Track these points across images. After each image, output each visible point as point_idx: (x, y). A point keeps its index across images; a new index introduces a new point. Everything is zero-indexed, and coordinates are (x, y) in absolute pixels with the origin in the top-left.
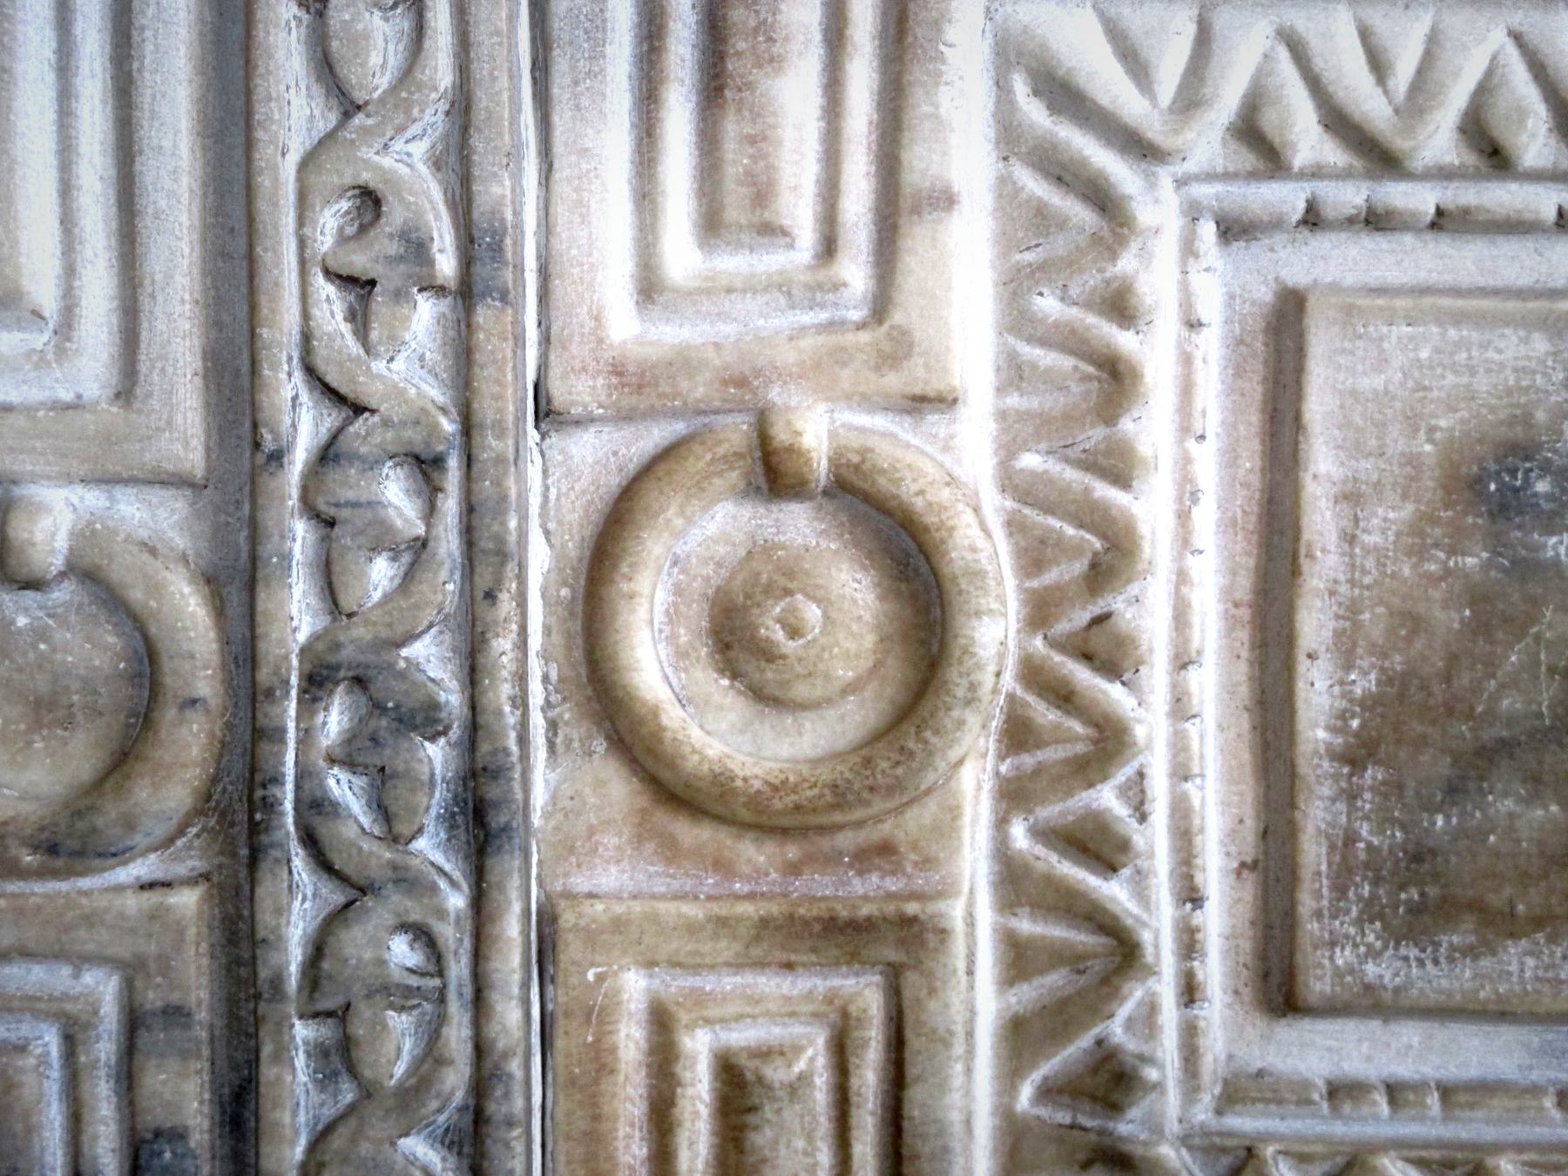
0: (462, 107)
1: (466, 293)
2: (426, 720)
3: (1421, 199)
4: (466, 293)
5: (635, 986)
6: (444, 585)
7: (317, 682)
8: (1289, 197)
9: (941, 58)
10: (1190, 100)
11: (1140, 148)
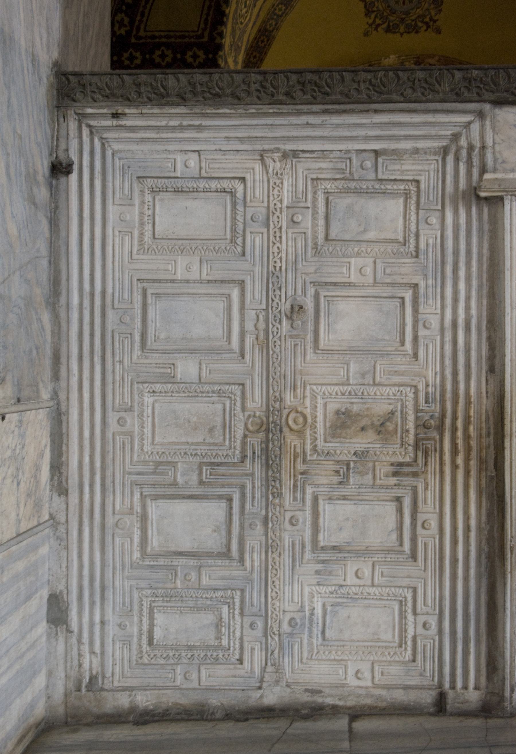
0: (281, 391)
1: (281, 402)
2: (278, 425)
3: (333, 397)
4: (281, 402)
5: (289, 441)
6: (279, 418)
7: (272, 423)
8: (326, 397)
10: (321, 391)
11: (318, 394)
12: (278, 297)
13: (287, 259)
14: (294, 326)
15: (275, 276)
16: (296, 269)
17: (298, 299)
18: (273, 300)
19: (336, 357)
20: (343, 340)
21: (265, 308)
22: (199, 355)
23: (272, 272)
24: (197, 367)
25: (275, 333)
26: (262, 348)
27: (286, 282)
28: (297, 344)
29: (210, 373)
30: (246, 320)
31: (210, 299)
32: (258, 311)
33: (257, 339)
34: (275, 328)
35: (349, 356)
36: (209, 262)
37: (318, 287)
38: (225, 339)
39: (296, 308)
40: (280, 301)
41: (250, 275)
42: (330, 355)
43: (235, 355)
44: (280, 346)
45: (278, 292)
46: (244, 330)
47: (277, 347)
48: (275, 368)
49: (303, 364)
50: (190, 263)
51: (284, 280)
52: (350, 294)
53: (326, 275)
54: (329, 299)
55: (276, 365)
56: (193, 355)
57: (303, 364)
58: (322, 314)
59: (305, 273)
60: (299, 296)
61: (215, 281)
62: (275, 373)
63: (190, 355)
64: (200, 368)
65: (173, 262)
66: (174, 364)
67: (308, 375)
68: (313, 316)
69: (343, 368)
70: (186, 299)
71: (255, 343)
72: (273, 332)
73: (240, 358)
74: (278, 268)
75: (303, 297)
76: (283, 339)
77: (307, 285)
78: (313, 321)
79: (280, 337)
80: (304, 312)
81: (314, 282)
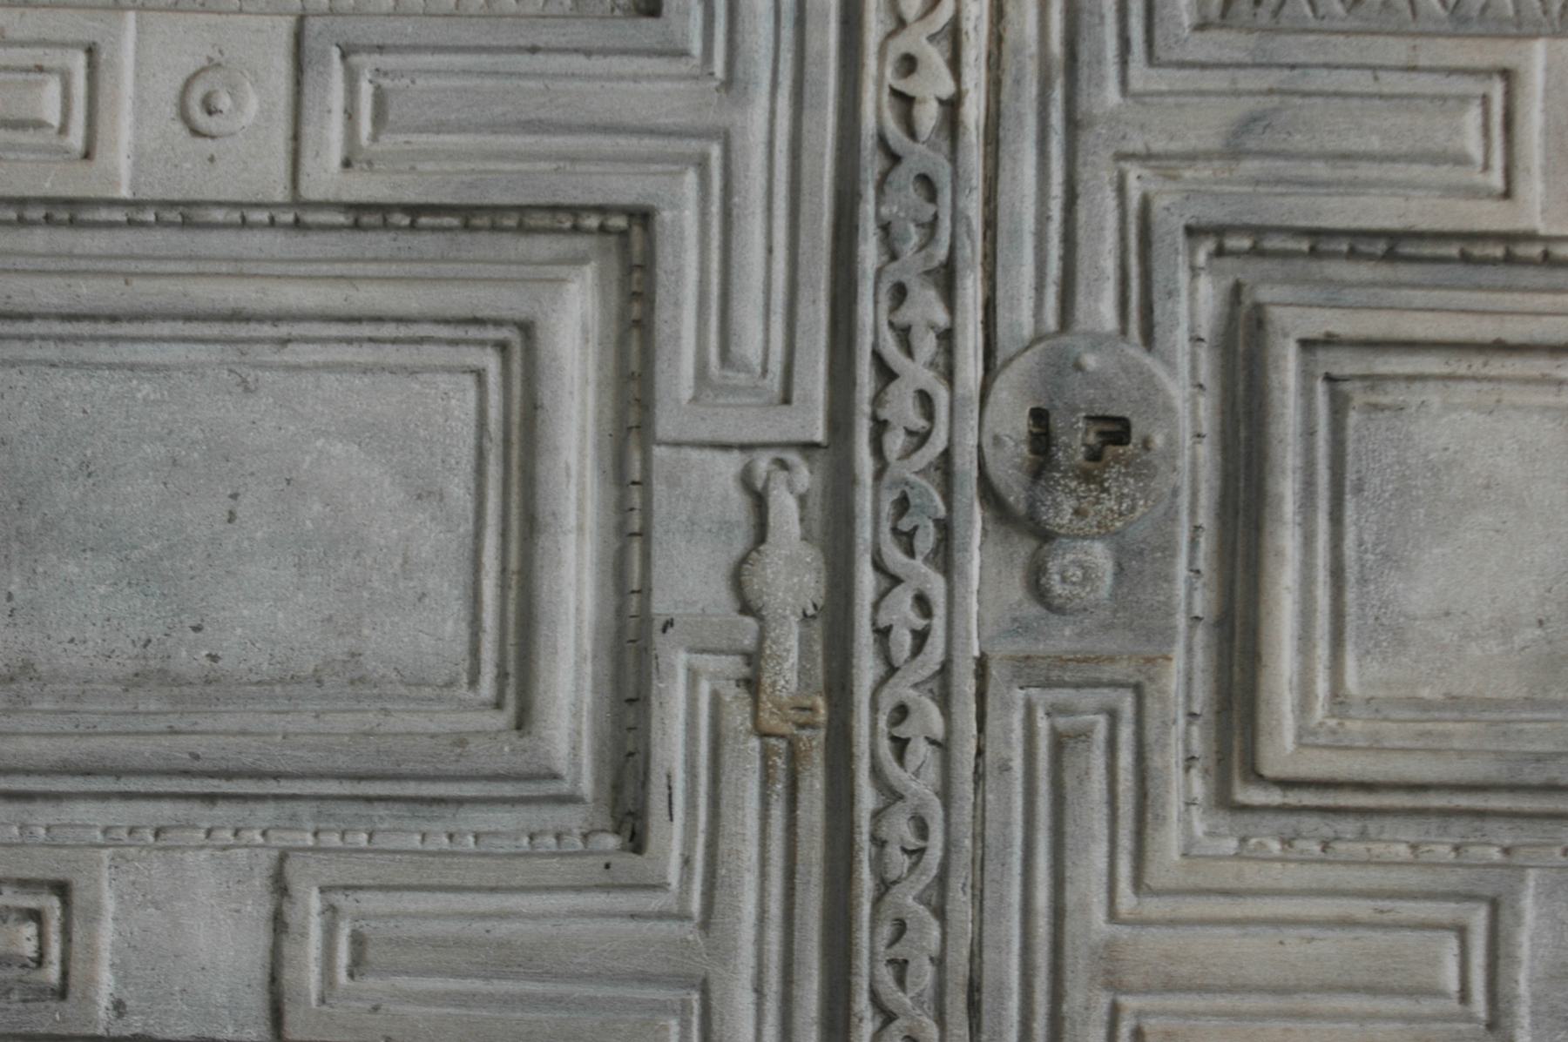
12: (927, 346)
13: (997, 39)
14: (1057, 588)
15: (904, 175)
16: (1073, 124)
17: (1091, 361)
18: (886, 373)
19: (1395, 841)
20: (1456, 704)
21: (819, 435)
22: (267, 812)
23: (882, 140)
24: (258, 908)
25: (902, 641)
26: (793, 756)
27: (990, 224)
28: (1084, 735)
29: (357, 966)
30: (657, 533)
31: (367, 354)
32: (763, 462)
33: (751, 685)
34: (902, 601)
35: (1505, 834)
36: (366, 63)
37: (1250, 271)
38: (487, 687)
39: (1075, 441)
40: (949, 375)
41: (702, 164)
42: (1349, 826)
43: (572, 818)
44: (943, 746)
45: (926, 307)
46: (645, 617)
47: (920, 751)
48: (901, 927)
49: (1126, 899)
50: (213, 65)
51: (974, 207)
52: (1514, 330)
53: (1320, 170)
54: (1347, 364)
55: (907, 899)
56: (222, 810)
57: (1126, 899)
58: (1286, 489)
59: (1146, 157)
60: (1097, 341)
61: (415, 210)
62: (900, 967)
63: (197, 810)
64: (279, 923)
65: (79, 62)
66: (62, 890)
67: (1170, 986)
68: (1207, 500)
69: (1462, 932)
70: (177, 352)
71: (738, 715)
72: (883, 634)
73: (611, 842)
74: (928, 116)
75: (1133, 350)
76: (966, 685)
77: (1160, 250)
78: (1205, 544)
79: (945, 670)
80: (1142, 470)
81: (1220, 231)
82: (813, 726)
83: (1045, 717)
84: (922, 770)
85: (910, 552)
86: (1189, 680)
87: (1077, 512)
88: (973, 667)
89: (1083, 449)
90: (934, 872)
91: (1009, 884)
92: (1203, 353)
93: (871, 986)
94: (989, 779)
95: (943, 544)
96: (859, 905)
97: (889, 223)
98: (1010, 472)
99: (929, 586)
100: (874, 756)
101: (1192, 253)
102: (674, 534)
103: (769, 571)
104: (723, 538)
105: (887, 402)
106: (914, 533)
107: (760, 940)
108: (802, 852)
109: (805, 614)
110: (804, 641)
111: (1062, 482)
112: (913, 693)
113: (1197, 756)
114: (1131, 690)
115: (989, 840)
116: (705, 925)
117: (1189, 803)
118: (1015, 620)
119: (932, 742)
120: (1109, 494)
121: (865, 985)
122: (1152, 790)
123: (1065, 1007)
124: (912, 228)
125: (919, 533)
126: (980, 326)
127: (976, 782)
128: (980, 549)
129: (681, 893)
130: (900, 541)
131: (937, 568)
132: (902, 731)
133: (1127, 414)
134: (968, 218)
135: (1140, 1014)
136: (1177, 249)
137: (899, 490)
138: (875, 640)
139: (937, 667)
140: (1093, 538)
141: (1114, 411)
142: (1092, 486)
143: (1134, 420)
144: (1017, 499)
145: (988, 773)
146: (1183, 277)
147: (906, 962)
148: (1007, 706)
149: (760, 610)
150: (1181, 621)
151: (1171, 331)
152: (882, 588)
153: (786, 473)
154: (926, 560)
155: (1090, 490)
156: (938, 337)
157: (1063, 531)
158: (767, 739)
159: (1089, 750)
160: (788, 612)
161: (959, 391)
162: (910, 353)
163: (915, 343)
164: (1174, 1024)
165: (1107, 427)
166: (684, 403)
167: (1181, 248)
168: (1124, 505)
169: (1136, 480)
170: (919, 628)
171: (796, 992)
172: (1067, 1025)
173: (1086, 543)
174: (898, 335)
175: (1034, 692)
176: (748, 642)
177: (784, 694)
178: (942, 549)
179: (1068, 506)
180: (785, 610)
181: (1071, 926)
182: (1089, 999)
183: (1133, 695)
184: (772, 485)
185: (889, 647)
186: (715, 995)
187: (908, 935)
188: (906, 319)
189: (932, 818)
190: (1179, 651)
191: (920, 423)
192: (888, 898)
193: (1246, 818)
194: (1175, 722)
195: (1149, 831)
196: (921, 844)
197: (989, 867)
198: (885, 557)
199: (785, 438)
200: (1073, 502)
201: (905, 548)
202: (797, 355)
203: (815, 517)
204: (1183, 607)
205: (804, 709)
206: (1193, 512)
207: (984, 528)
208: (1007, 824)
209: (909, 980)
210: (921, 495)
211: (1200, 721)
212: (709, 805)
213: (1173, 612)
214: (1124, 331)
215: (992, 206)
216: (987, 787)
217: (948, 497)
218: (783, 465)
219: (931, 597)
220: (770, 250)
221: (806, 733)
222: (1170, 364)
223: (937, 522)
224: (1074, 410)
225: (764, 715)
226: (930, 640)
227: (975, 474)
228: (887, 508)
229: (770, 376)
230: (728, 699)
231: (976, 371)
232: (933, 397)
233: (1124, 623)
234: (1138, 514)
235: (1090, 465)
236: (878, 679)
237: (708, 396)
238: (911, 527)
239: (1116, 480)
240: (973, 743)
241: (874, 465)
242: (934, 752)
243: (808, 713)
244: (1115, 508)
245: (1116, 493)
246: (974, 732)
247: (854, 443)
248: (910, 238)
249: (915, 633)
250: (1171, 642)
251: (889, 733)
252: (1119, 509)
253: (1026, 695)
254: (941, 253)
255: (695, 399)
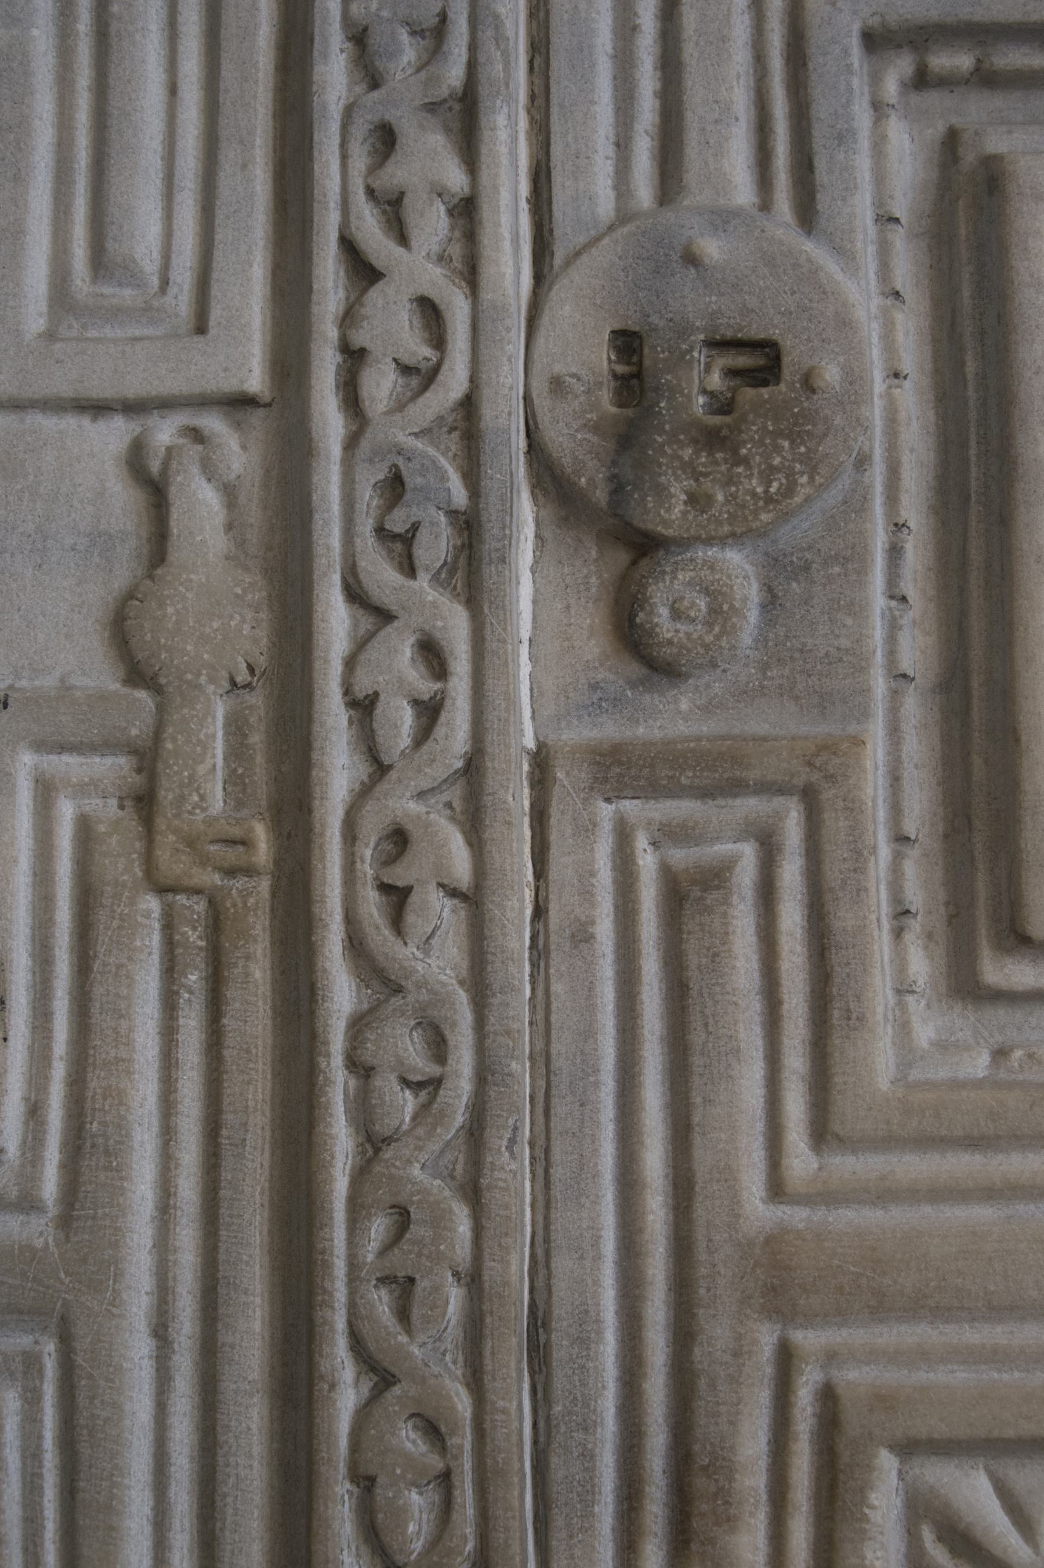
9: (865, 1519)
48: (403, 1218)
82: (249, 871)
83: (650, 849)
84: (433, 942)
85: (410, 570)
86: (895, 779)
87: (692, 499)
88: (526, 767)
89: (701, 400)
90: (460, 1119)
91: (594, 1139)
92: (899, 239)
93: (350, 1324)
94: (555, 957)
95: (466, 552)
96: (330, 1180)
97: (365, 29)
98: (579, 436)
99: (440, 624)
100: (351, 919)
101: (875, 80)
102: (13, 555)
103: (170, 610)
104: (97, 559)
105: (365, 318)
106: (414, 536)
107: (163, 1246)
108: (231, 1089)
109: (233, 683)
110: (236, 727)
111: (669, 451)
112: (414, 807)
113: (913, 910)
114: (795, 798)
115: (559, 1063)
116: (66, 1221)
117: (903, 990)
118: (594, 687)
119: (453, 893)
120: (748, 466)
121: (341, 1324)
122: (837, 969)
123: (697, 1351)
124: (404, 37)
125: (423, 536)
126: (524, 206)
127: (535, 965)
128: (533, 572)
129: (23, 1166)
130: (390, 551)
131: (455, 595)
132: (400, 875)
133: (775, 334)
134: (497, 17)
135: (831, 1357)
136: (849, 66)
137: (387, 463)
138: (351, 722)
139: (459, 764)
140: (722, 541)
141: (755, 332)
142: (719, 456)
143: (787, 343)
144: (591, 480)
145: (553, 947)
146: (863, 118)
147: (412, 1280)
148: (587, 830)
149: (154, 677)
150: (879, 685)
151: (844, 199)
152: (362, 632)
153: (200, 448)
154: (435, 578)
155: (716, 463)
156: (450, 213)
157: (670, 532)
158: (170, 896)
159: (726, 902)
160: (203, 679)
161: (486, 296)
162: (403, 240)
163: (411, 218)
164: (891, 1376)
165: (742, 360)
166: (28, 337)
167: (856, 65)
168: (775, 485)
169: (792, 442)
170: (426, 697)
171: (225, 1337)
172: (702, 1383)
173: (712, 552)
174: (384, 212)
175: (630, 807)
176: (138, 730)
177: (200, 816)
178: (462, 561)
179: (678, 490)
180: (199, 674)
181: (701, 1212)
182: (739, 1337)
183: (802, 808)
184: (174, 465)
185: (372, 731)
186: (82, 1345)
187: (416, 1231)
188: (395, 182)
189: (454, 1025)
190: (877, 731)
191: (422, 352)
192: (378, 1168)
193: (1001, 1014)
194: (874, 850)
195: (836, 1040)
196: (434, 1070)
197: (559, 1108)
198: (362, 576)
199: (195, 387)
200: (689, 483)
201: (400, 563)
202: (218, 254)
203: (252, 520)
204: (879, 658)
205: (232, 842)
206: (892, 499)
207: (538, 536)
208: (589, 1033)
209: (416, 1313)
210: (423, 471)
211: (913, 853)
212: (71, 1012)
213: (863, 664)
214: (766, 205)
215: (542, 15)
216: (552, 971)
217: (472, 477)
218: (196, 435)
219: (443, 643)
220: (173, 90)
221: (240, 883)
222: (844, 253)
223: (453, 514)
224: (684, 330)
225: (163, 855)
226: (443, 717)
227: (522, 443)
228: (367, 497)
229: (172, 290)
230: (102, 828)
231: (518, 273)
232: (442, 307)
233: (781, 686)
234: (798, 499)
235: (717, 420)
236: (357, 787)
237: (70, 327)
238: (408, 526)
239: (761, 443)
240: (528, 895)
241: (346, 427)
242: (454, 911)
243: (241, 848)
244: (759, 490)
245: (760, 465)
246: (530, 877)
247: (309, 388)
248: (401, 51)
249: (416, 703)
250: (865, 714)
251: (376, 878)
252: (766, 492)
253: (617, 811)
254: (454, 74)
255: (50, 336)
